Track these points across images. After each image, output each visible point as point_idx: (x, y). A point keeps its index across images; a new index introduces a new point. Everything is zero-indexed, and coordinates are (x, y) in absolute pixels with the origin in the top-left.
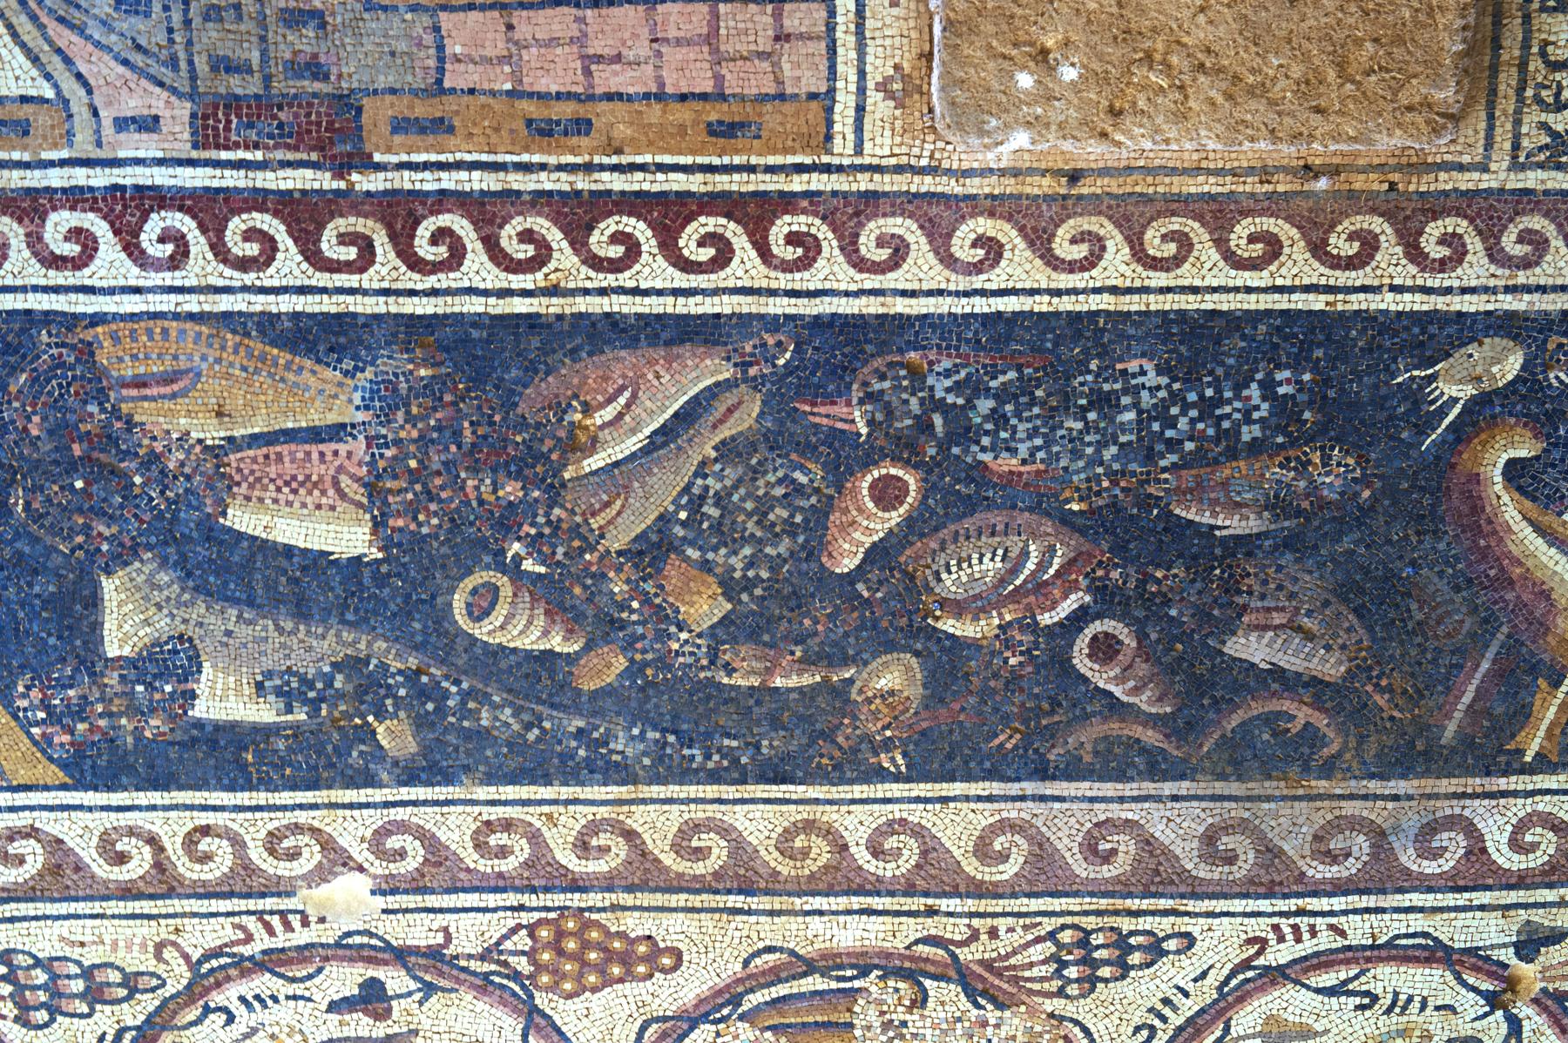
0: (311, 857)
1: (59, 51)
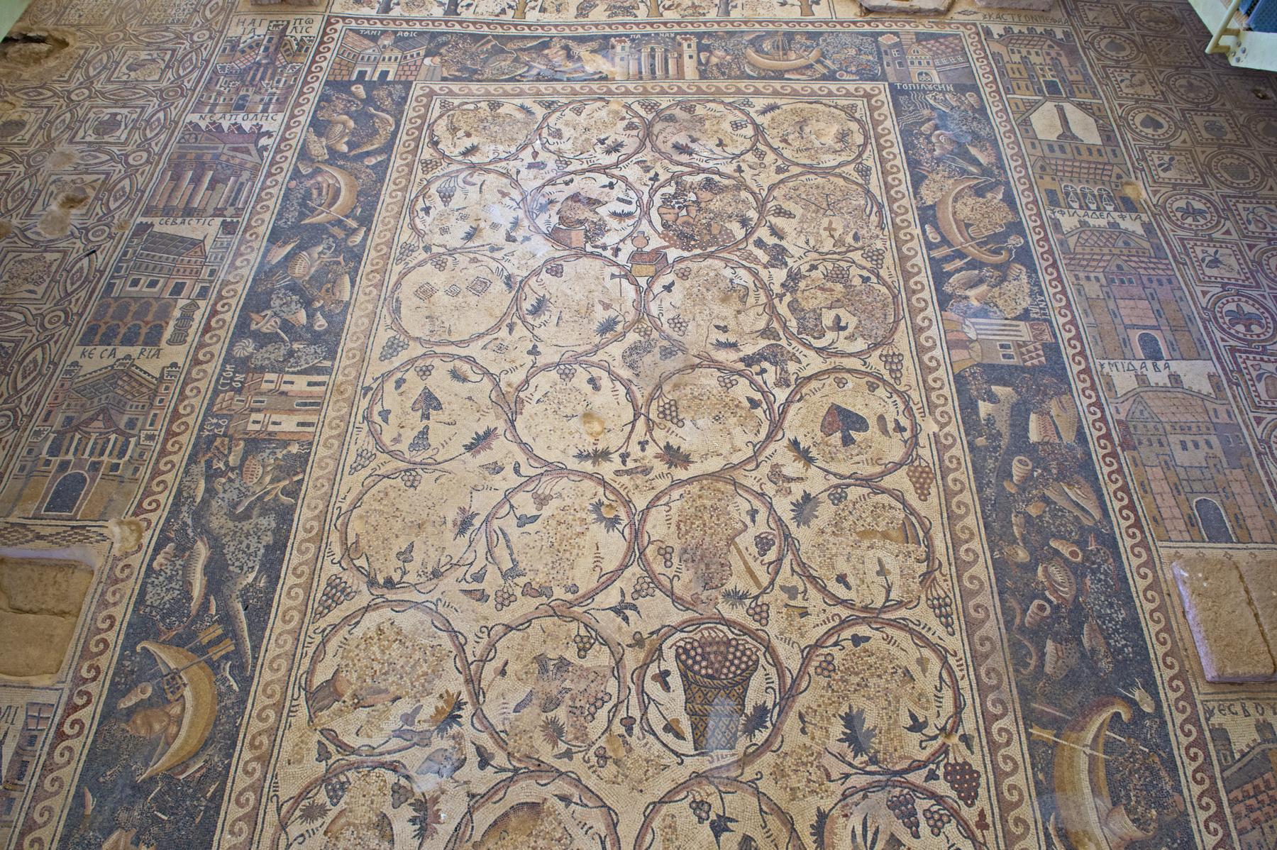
0: (942, 420)
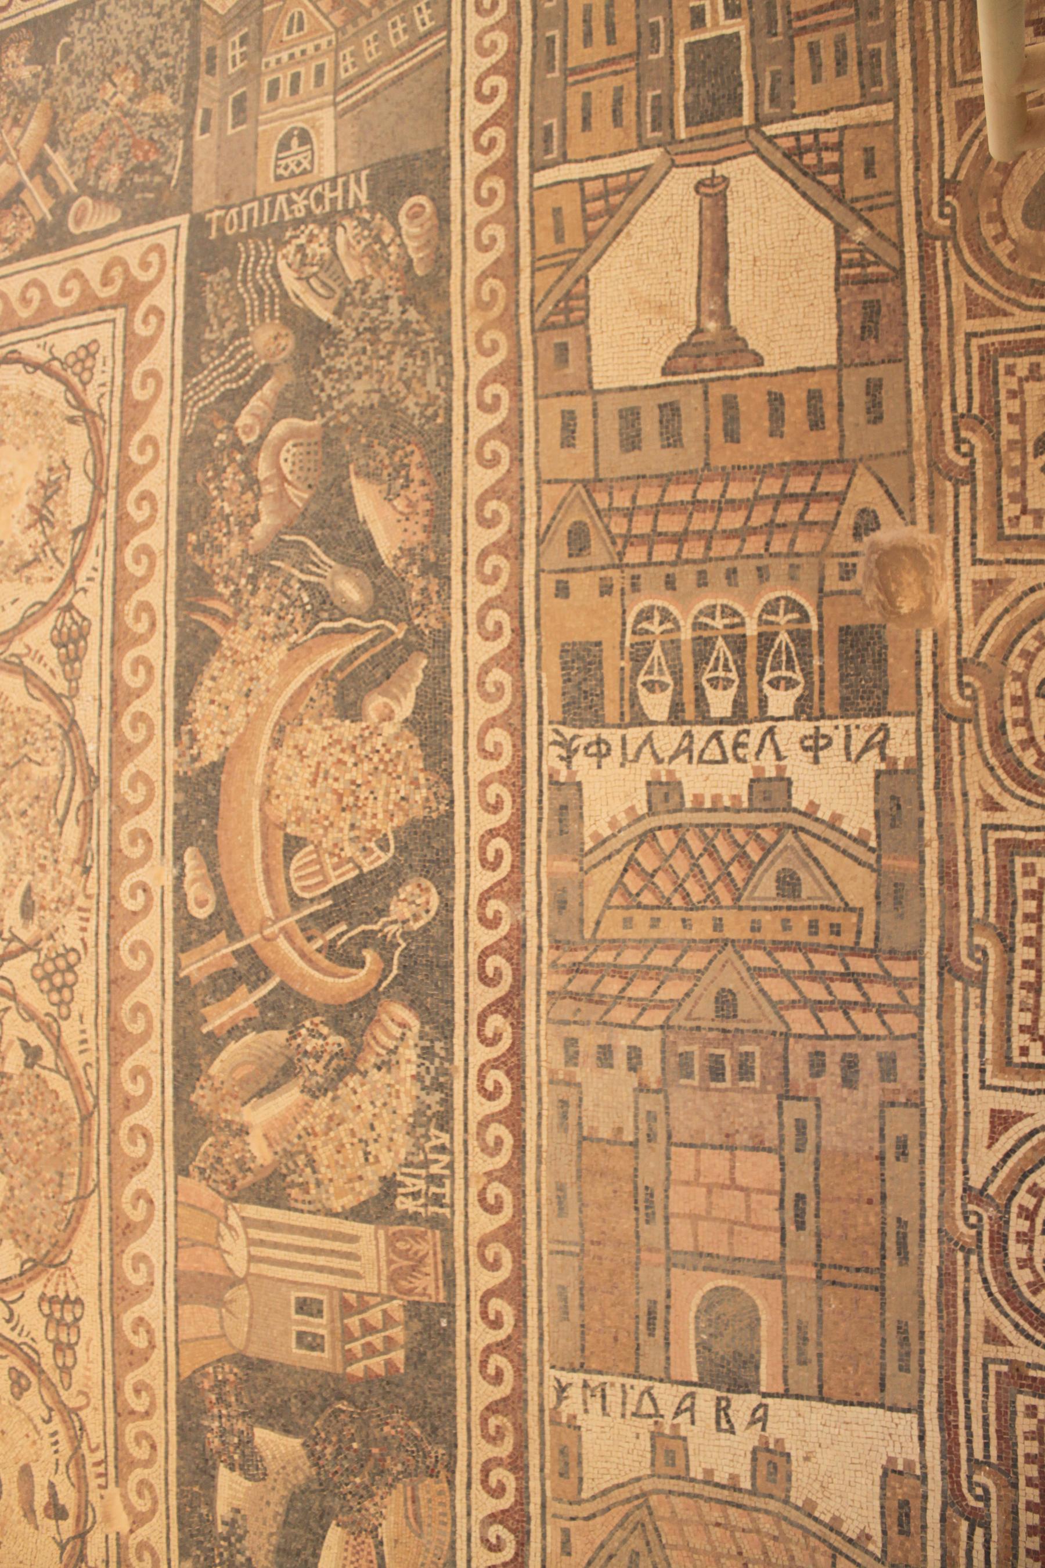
1: (609, 1509)
